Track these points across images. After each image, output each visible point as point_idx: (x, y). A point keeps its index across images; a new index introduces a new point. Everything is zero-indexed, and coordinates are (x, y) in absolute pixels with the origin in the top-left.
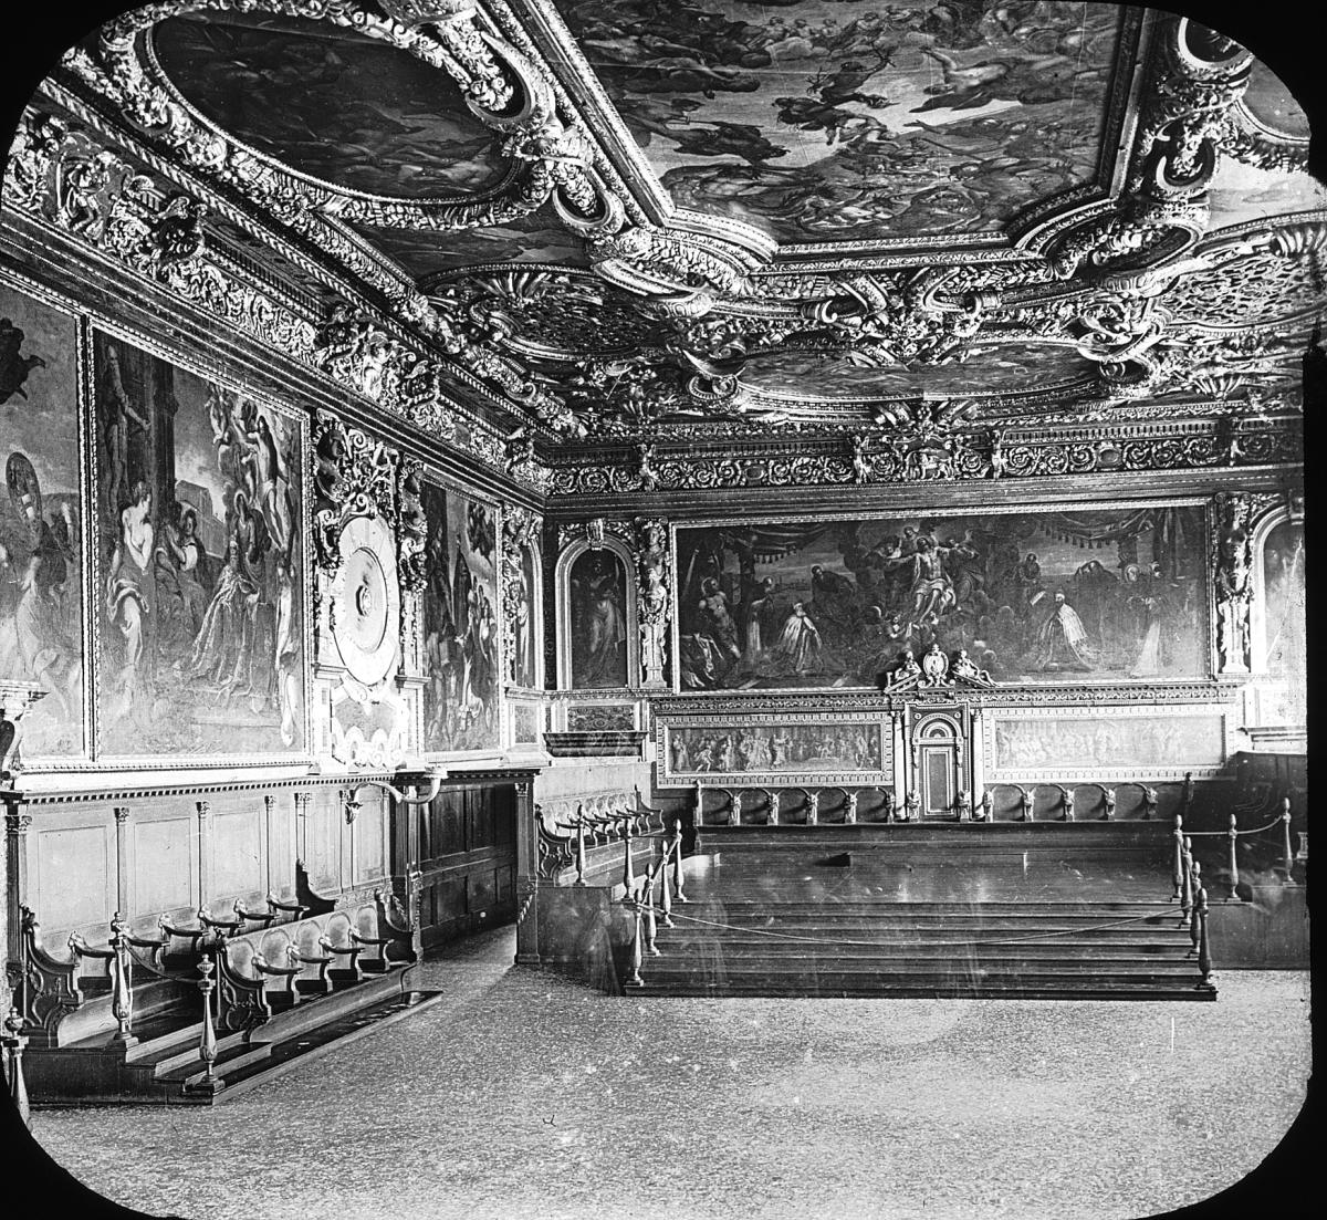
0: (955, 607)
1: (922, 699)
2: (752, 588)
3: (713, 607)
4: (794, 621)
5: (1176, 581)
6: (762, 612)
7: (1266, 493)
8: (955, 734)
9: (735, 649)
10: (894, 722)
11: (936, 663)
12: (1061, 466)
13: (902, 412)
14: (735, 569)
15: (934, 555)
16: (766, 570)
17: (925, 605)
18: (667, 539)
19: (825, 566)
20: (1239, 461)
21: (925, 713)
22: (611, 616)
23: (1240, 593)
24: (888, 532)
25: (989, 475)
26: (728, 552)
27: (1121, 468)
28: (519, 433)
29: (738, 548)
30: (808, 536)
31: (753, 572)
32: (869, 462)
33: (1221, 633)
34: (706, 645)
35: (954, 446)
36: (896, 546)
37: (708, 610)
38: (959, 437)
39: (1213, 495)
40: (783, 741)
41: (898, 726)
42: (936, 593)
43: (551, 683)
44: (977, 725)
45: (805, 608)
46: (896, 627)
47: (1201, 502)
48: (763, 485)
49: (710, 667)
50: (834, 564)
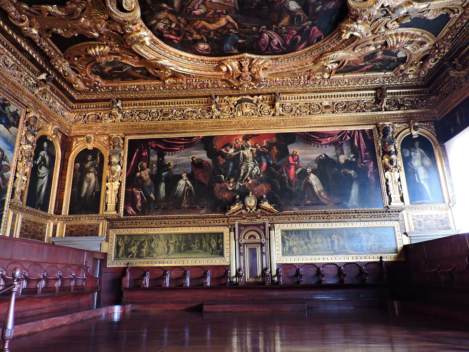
0: (259, 175)
1: (244, 219)
2: (162, 166)
3: (143, 175)
4: (182, 182)
5: (363, 163)
6: (167, 178)
7: (399, 123)
8: (261, 238)
9: (152, 195)
10: (230, 231)
11: (251, 201)
12: (306, 112)
13: (235, 64)
14: (154, 158)
15: (249, 151)
16: (169, 158)
17: (245, 174)
18: (123, 144)
19: (197, 157)
20: (386, 110)
21: (246, 226)
22: (93, 180)
23: (396, 167)
24: (228, 141)
25: (274, 115)
26: (152, 151)
27: (333, 112)
28: (43, 76)
29: (157, 148)
30: (189, 143)
31: (163, 159)
32: (219, 110)
33: (387, 186)
34: (138, 194)
35: (257, 102)
36: (231, 147)
37: (141, 177)
38: (260, 97)
39: (376, 124)
40: (173, 242)
41: (232, 233)
42: (250, 169)
43: (58, 210)
44: (272, 232)
45: (188, 176)
46: (231, 185)
47: (371, 127)
48: (170, 119)
49: (139, 204)
50: (202, 155)
